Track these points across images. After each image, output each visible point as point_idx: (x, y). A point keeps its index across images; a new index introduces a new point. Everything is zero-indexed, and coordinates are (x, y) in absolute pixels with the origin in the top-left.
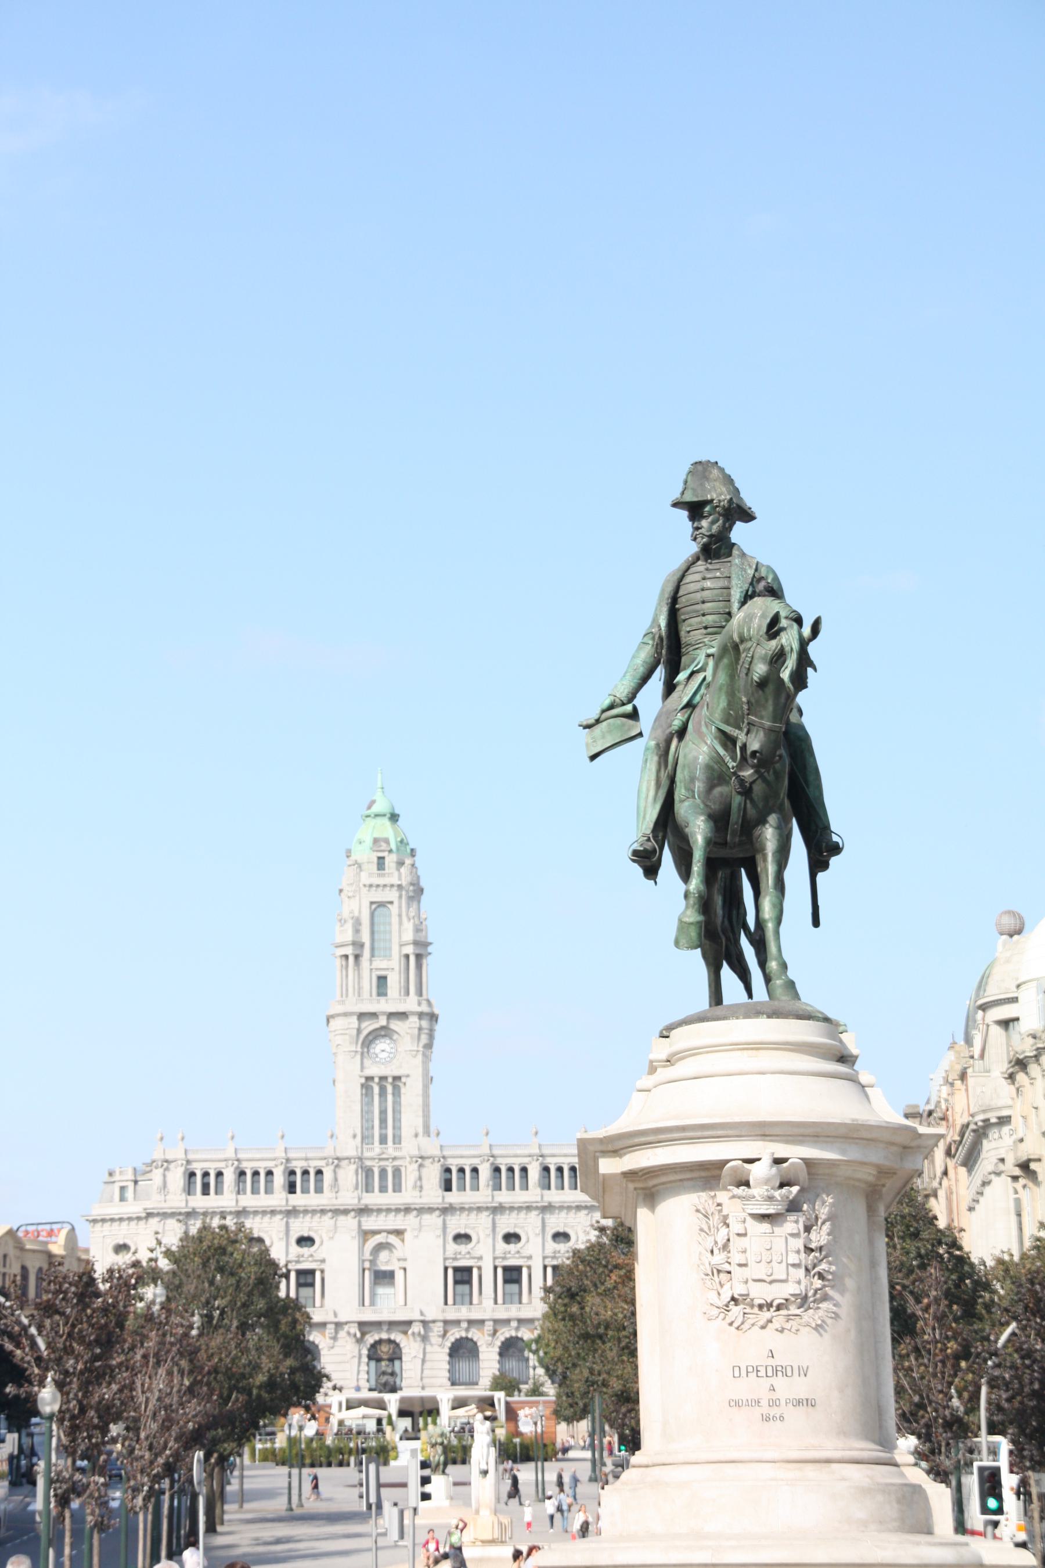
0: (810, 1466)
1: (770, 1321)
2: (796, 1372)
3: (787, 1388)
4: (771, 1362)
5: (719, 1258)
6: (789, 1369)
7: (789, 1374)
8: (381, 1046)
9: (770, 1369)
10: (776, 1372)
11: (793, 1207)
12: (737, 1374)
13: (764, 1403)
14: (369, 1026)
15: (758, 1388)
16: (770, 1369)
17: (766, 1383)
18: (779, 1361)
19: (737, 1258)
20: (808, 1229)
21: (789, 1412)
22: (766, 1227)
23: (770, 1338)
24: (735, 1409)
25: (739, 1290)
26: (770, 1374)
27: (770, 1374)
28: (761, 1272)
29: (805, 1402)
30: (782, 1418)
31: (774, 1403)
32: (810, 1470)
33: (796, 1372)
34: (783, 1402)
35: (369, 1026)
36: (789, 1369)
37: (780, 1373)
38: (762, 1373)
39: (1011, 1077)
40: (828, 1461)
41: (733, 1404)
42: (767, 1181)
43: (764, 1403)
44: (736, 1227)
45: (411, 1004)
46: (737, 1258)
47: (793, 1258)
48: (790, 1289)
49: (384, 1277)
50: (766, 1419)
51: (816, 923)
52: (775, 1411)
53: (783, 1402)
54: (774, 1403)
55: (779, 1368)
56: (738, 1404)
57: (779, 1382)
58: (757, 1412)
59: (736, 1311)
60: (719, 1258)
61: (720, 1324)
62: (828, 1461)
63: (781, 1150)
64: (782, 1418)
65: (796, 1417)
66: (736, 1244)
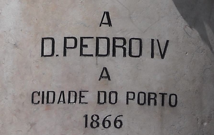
2: (147, 49)
4: (105, 31)
6: (135, 45)
7: (135, 52)
9: (103, 44)
10: (112, 47)
12: (48, 50)
13: (90, 97)
15: (83, 72)
16: (103, 44)
18: (120, 29)
24: (42, 107)
26: (103, 50)
27: (103, 50)
29: (159, 99)
30: (118, 123)
31: (106, 98)
33: (147, 49)
34: (122, 98)
36: (135, 45)
37: (119, 51)
38: (90, 49)
41: (37, 98)
43: (90, 97)
52: (107, 112)
53: (122, 98)
54: (106, 98)
55: (119, 43)
56: (43, 98)
58: (78, 112)
64: (118, 123)
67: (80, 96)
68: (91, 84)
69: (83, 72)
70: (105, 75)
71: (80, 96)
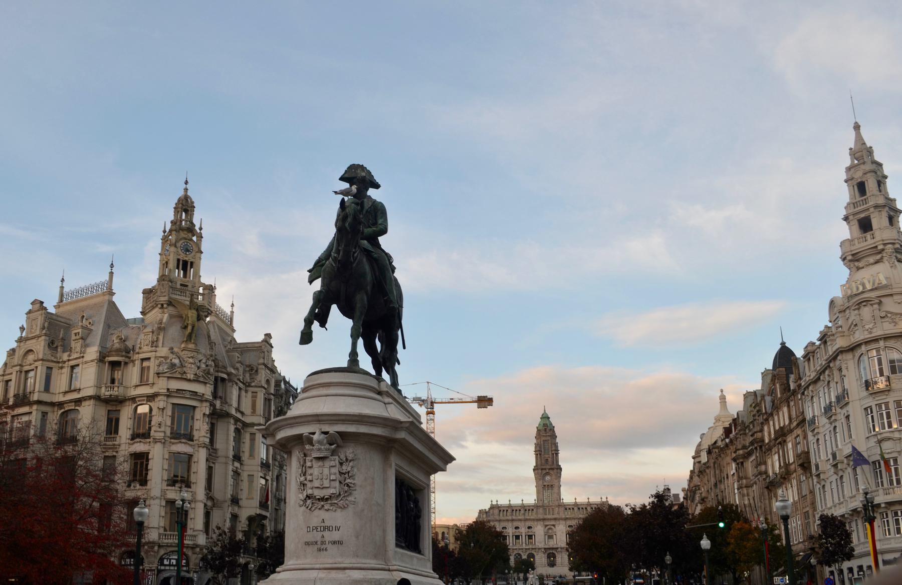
0: (334, 571)
1: (323, 506)
3: (329, 536)
4: (323, 524)
5: (302, 478)
8: (548, 478)
11: (334, 453)
13: (319, 543)
14: (544, 472)
15: (317, 536)
17: (320, 534)
18: (327, 524)
19: (309, 478)
20: (341, 464)
21: (329, 546)
22: (320, 463)
23: (323, 514)
25: (310, 492)
28: (317, 483)
31: (323, 543)
32: (334, 574)
35: (544, 472)
39: (699, 476)
40: (345, 569)
42: (319, 442)
43: (319, 543)
44: (308, 464)
45: (555, 466)
46: (309, 478)
47: (333, 477)
48: (332, 491)
49: (550, 537)
50: (320, 550)
51: (404, 348)
52: (324, 547)
54: (323, 543)
56: (307, 544)
57: (326, 534)
58: (316, 547)
59: (309, 501)
60: (302, 478)
61: (303, 508)
62: (345, 569)
63: (326, 428)
65: (333, 550)
66: (309, 471)
67: (316, 543)
68: (319, 539)
69: (317, 536)
70: (323, 537)
71: (316, 543)
